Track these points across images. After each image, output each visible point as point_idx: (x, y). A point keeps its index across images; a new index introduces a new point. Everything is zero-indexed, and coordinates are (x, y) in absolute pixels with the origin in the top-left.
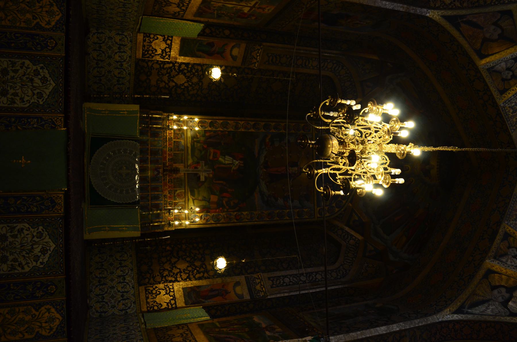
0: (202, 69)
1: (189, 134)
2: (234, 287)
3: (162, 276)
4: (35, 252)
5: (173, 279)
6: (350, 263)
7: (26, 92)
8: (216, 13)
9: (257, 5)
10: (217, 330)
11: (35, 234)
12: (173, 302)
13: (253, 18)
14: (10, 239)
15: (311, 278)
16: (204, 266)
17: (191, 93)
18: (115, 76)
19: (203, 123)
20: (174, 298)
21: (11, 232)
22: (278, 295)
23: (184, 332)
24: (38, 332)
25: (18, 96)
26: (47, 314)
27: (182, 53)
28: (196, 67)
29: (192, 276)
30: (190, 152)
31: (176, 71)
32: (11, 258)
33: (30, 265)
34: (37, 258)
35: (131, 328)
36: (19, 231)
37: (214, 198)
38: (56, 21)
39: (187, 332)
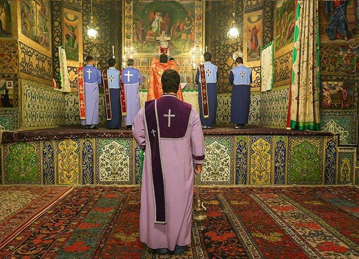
0: (86, 44)
2: (251, 22)
8: (44, 33)
11: (207, 152)
12: (256, 69)
14: (210, 166)
16: (233, 45)
17: (105, 53)
20: (254, 68)
21: (206, 165)
23: (280, 62)
24: (268, 152)
27: (76, 59)
30: (149, 54)
32: (221, 166)
34: (223, 152)
35: (271, 98)
37: (184, 36)
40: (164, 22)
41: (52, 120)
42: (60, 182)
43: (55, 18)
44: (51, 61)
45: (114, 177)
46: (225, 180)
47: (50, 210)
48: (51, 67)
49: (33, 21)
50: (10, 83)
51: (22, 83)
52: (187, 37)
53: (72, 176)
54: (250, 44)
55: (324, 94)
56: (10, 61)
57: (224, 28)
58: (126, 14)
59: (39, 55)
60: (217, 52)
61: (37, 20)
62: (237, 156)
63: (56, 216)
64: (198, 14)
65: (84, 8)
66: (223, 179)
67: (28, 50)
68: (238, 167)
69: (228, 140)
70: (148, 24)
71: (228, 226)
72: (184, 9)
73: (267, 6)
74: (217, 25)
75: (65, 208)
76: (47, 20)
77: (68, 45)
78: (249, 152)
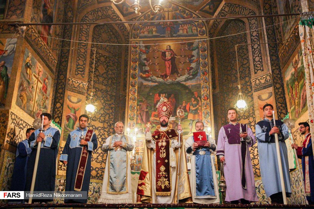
0: (88, 127)
3: (254, 158)
5: (256, 149)
6: (244, 10)
8: (43, 110)
9: (37, 76)
10: (297, 107)
13: (47, 81)
15: (256, 40)
18: (93, 194)
19: (130, 125)
22: (270, 64)
35: (296, 178)
37: (191, 116)
43: (57, 100)
49: (31, 95)
51: (6, 155)
52: (194, 117)
58: (130, 97)
61: (37, 96)
64: (205, 95)
70: (153, 105)
72: (190, 90)
73: (276, 83)
76: (47, 98)
77: (68, 126)
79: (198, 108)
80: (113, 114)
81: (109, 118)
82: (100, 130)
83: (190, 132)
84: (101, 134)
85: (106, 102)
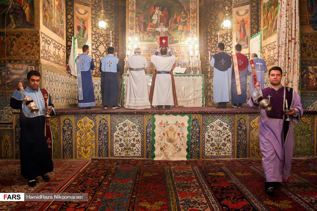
0: (94, 34)
1: (139, 43)
4: (221, 129)
7: (132, 134)
8: (60, 24)
11: (211, 129)
14: (213, 142)
16: (224, 35)
19: (131, 34)
21: (210, 141)
25: (134, 139)
26: (255, 124)
28: (93, 38)
29: (229, 44)
31: (97, 51)
32: (223, 141)
33: (228, 132)
34: (225, 129)
36: (210, 137)
37: (180, 28)
38: (90, 120)
39: (268, 47)
40: (163, 15)
41: (65, 101)
42: (78, 157)
44: (65, 49)
45: (127, 152)
46: (227, 154)
47: (74, 181)
48: (65, 54)
50: (32, 68)
52: (183, 28)
53: (89, 152)
54: (239, 35)
55: (310, 77)
56: (32, 48)
57: (214, 20)
59: (56, 44)
60: (208, 41)
61: (55, 14)
62: (238, 132)
63: (81, 187)
64: (193, 9)
65: (93, 3)
66: (225, 153)
67: (48, 40)
68: (239, 142)
69: (230, 118)
70: (149, 17)
71: (240, 195)
72: (180, 4)
74: (208, 18)
75: (87, 180)
76: (62, 13)
77: (79, 35)
78: (248, 128)
79: (187, 20)
80: (114, 22)
81: (111, 26)
82: (104, 37)
83: (180, 41)
84: (105, 40)
85: (108, 12)
